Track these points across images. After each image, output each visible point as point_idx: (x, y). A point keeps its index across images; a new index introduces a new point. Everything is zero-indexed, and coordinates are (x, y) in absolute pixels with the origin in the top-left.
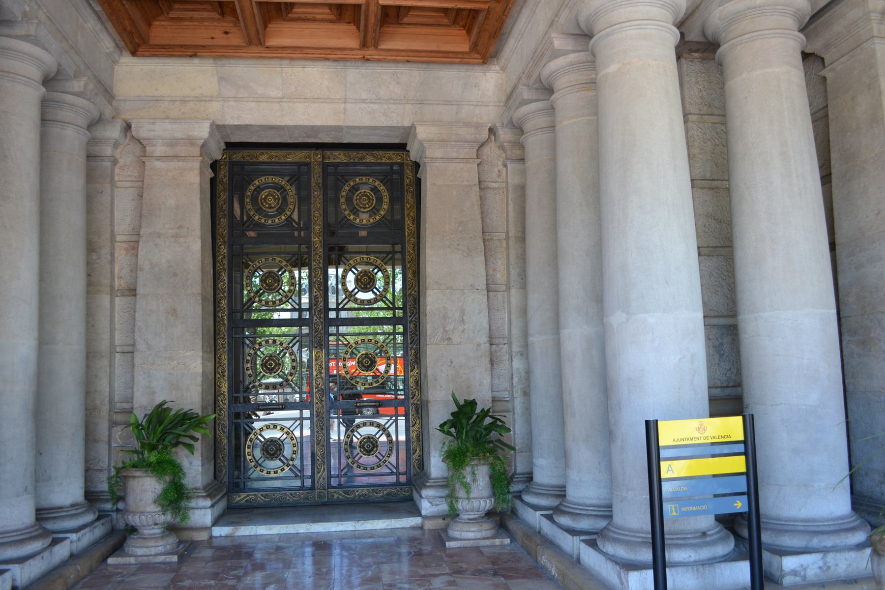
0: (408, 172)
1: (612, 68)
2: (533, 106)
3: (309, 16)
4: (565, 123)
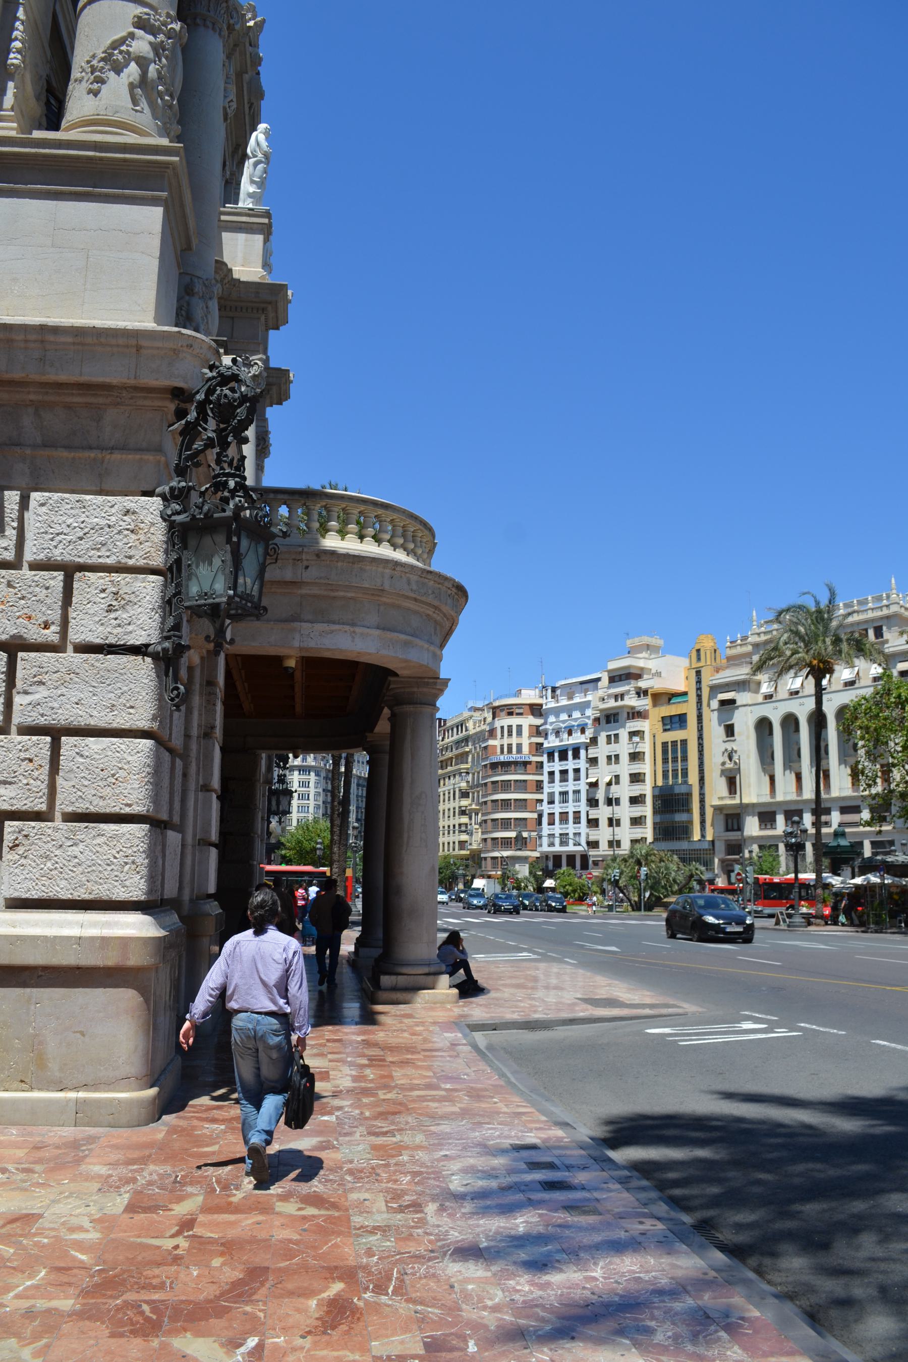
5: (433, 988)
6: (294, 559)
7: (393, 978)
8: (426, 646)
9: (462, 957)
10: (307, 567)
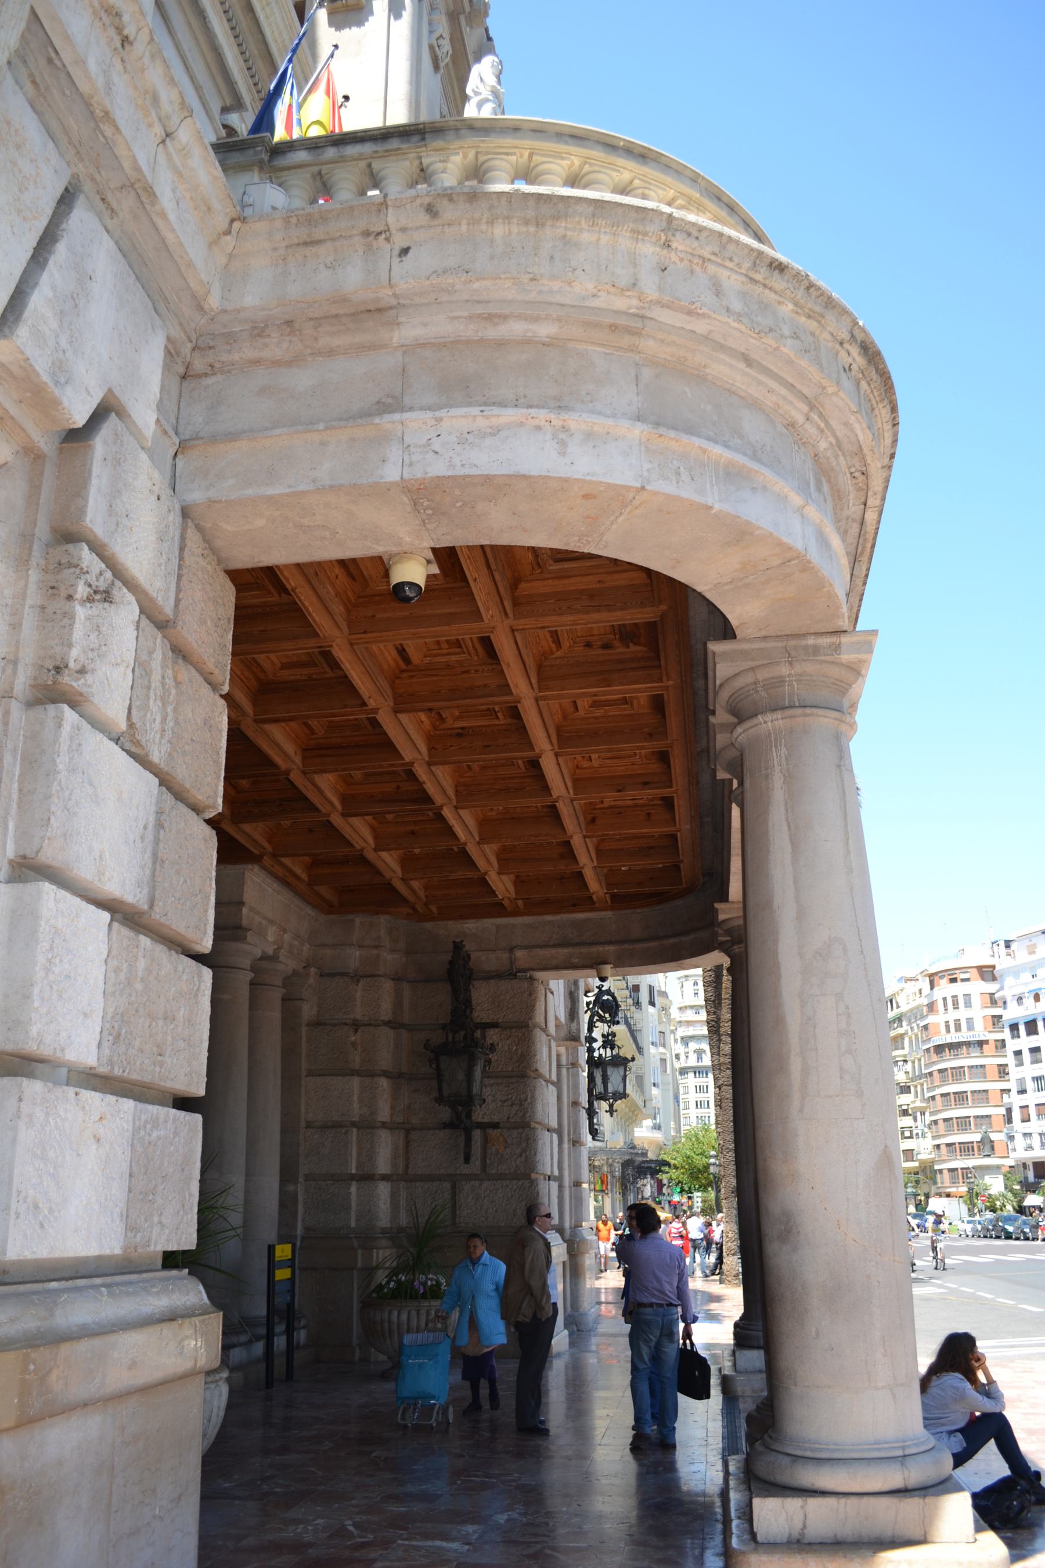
5: (922, 1540)
6: (367, 234)
7: (793, 1504)
8: (796, 500)
9: (989, 1407)
10: (405, 251)
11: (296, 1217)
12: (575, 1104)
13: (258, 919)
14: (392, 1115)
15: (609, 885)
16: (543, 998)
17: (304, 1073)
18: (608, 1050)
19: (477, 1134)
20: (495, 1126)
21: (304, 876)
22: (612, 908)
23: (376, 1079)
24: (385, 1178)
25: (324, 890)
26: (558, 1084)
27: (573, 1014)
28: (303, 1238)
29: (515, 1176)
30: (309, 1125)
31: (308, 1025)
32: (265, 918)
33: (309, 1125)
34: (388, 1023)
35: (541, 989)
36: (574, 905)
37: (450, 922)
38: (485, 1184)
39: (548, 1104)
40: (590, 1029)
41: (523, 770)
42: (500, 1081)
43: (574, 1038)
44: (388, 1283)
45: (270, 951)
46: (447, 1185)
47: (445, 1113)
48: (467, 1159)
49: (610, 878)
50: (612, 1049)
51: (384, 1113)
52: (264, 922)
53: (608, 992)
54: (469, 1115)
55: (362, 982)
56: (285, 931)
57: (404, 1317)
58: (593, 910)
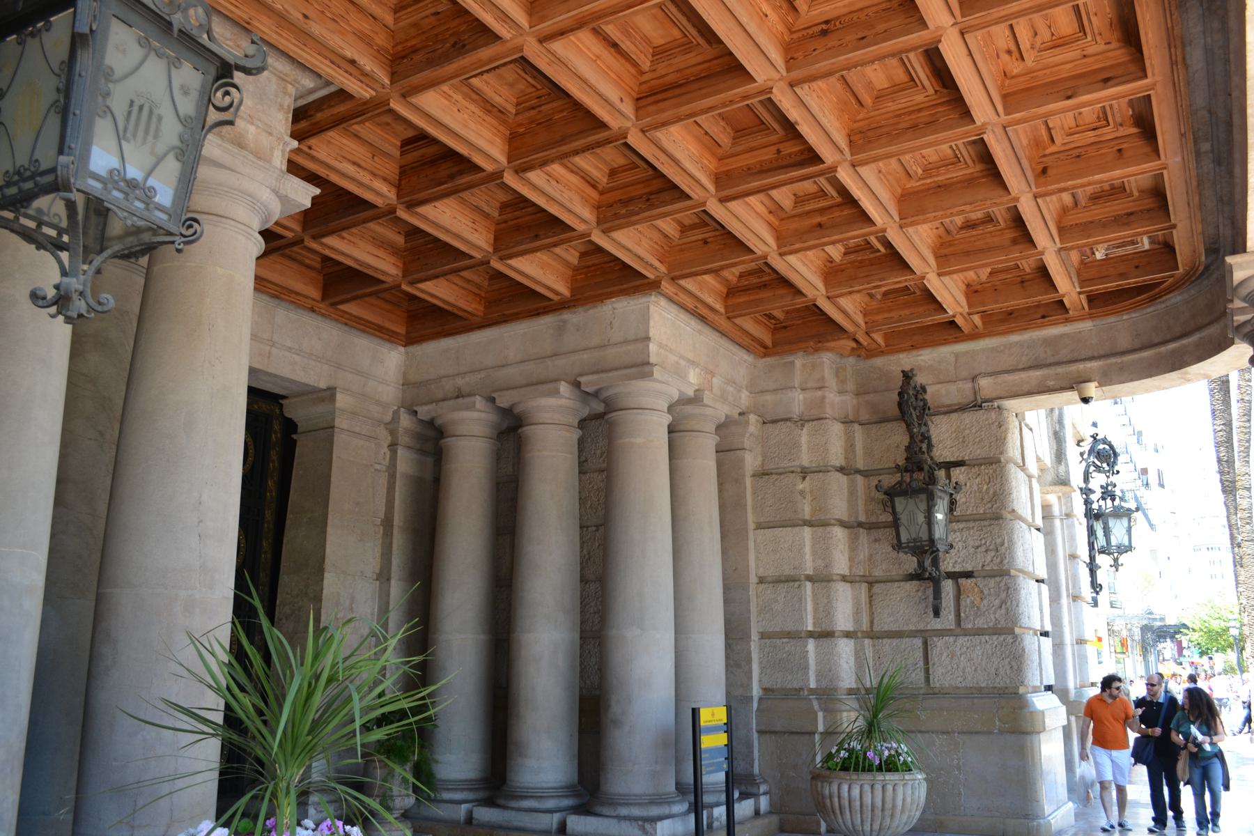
0: (276, 426)
1: (639, 440)
2: (475, 415)
3: (299, 258)
4: (545, 453)
11: (750, 678)
12: (1073, 557)
13: (672, 358)
14: (851, 568)
15: (1083, 282)
16: (1017, 432)
17: (751, 526)
18: (1109, 501)
19: (948, 586)
20: (968, 575)
21: (719, 306)
22: (1091, 317)
23: (829, 529)
24: (848, 635)
25: (747, 324)
26: (1048, 532)
27: (1060, 456)
28: (760, 699)
29: (996, 631)
30: (761, 581)
31: (753, 476)
32: (682, 357)
33: (761, 581)
34: (841, 470)
35: (1013, 423)
36: (1043, 317)
37: (901, 356)
38: (962, 640)
39: (1030, 550)
40: (1086, 480)
41: (931, 91)
42: (971, 524)
43: (1064, 482)
44: (838, 751)
45: (690, 393)
46: (918, 642)
47: (911, 563)
48: (937, 613)
49: (1086, 272)
50: (1113, 500)
51: (841, 565)
52: (683, 363)
53: (1105, 441)
54: (935, 562)
55: (806, 425)
56: (712, 374)
57: (856, 792)
58: (1067, 321)
